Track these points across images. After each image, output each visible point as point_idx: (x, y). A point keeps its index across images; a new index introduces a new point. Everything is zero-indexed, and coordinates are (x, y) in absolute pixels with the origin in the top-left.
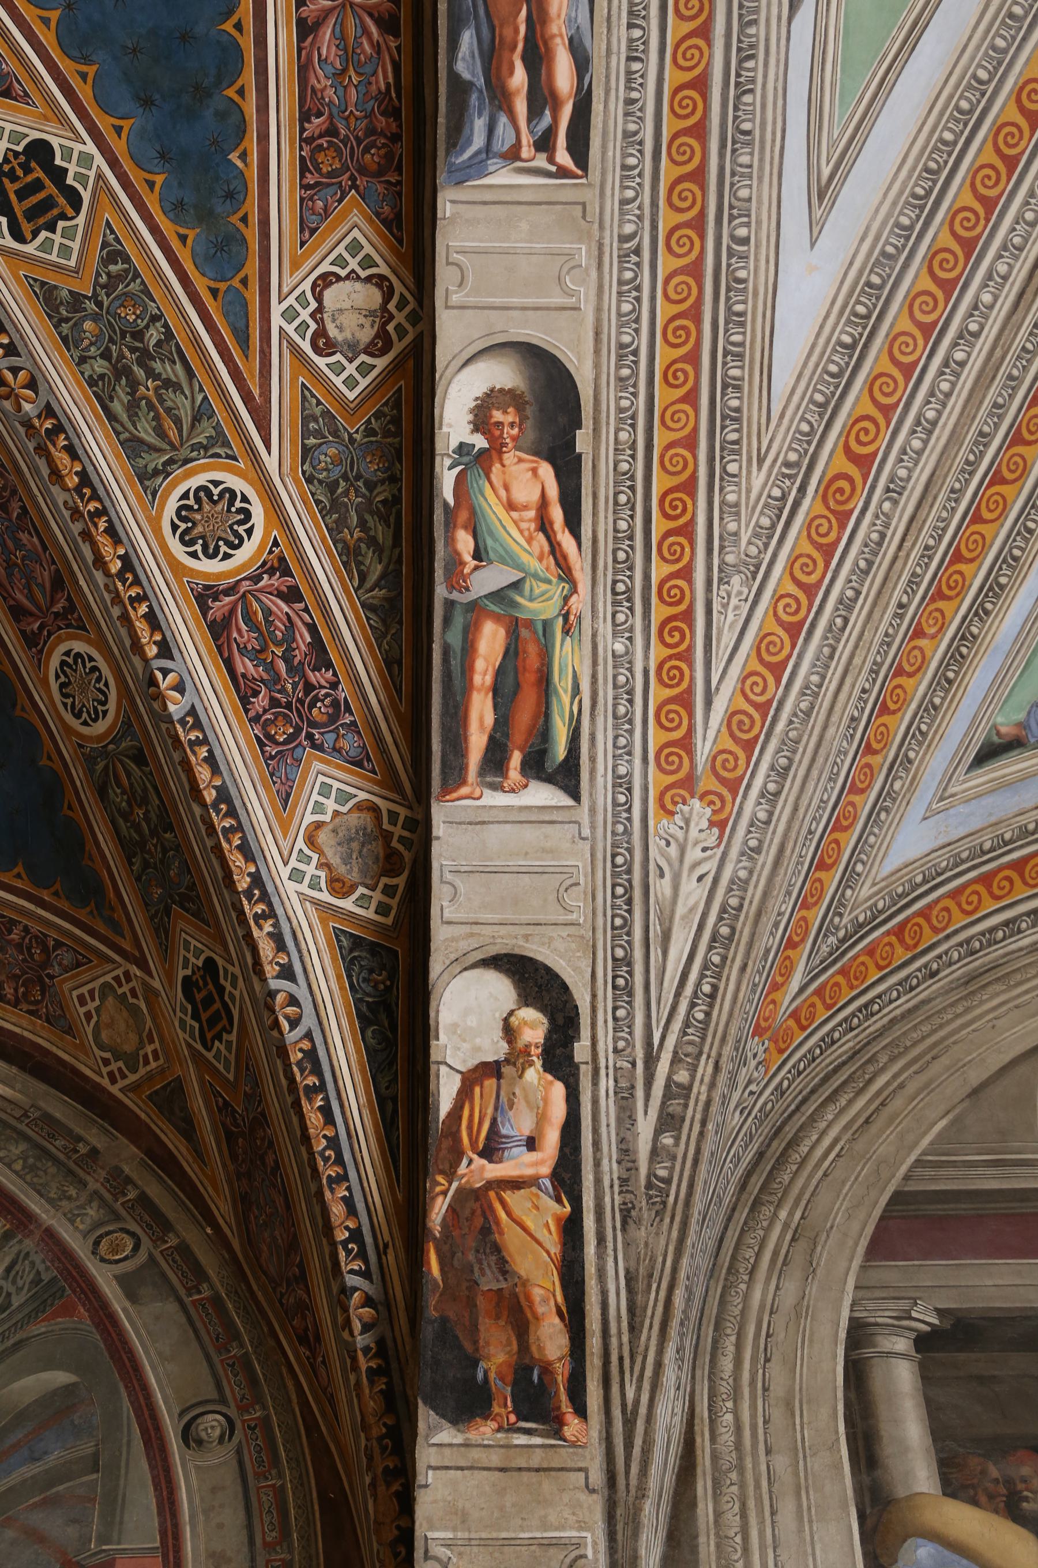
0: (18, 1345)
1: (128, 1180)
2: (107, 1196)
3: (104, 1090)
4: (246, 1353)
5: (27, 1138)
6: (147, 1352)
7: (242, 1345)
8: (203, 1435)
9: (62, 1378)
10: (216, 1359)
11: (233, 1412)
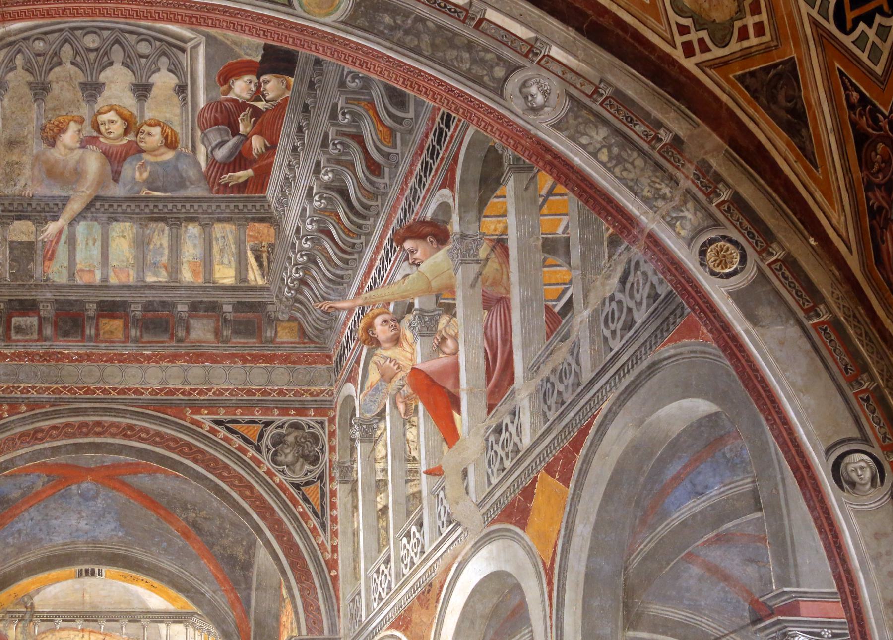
0: (653, 367)
1: (718, 178)
2: (700, 195)
3: (674, 62)
4: (878, 387)
5: (605, 122)
6: (779, 382)
7: (872, 378)
8: (854, 475)
9: (703, 407)
10: (850, 393)
11: (877, 452)
